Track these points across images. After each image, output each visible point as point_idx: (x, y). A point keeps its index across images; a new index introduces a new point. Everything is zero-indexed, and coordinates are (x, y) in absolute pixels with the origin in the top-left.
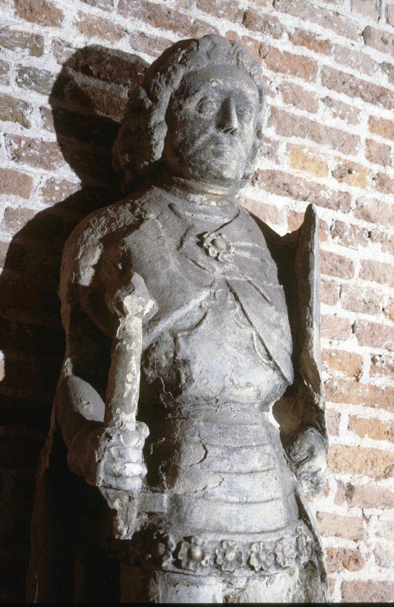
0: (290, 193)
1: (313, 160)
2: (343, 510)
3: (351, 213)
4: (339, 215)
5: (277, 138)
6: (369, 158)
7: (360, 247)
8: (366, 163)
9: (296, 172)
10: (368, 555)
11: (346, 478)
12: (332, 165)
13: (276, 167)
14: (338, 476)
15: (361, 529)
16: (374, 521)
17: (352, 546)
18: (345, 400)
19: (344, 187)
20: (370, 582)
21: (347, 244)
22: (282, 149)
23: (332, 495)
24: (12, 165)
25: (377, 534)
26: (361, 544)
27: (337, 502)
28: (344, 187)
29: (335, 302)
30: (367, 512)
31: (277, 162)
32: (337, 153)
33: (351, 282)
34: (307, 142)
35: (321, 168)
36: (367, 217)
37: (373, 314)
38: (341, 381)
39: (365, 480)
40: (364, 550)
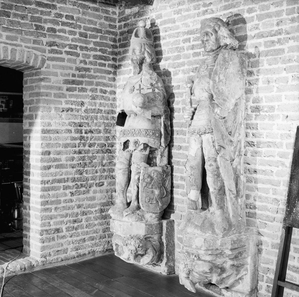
0: (263, 37)
1: (269, 24)
3: (283, 34)
4: (279, 37)
5: (259, 23)
6: (287, 14)
7: (286, 44)
8: (286, 17)
9: (266, 30)
12: (275, 23)
13: (259, 31)
14: (283, 113)
17: (288, 132)
19: (280, 27)
21: (282, 44)
22: (261, 25)
24: (203, 57)
28: (280, 27)
32: (277, 18)
33: (284, 55)
34: (267, 19)
35: (272, 25)
36: (288, 34)
37: (291, 63)
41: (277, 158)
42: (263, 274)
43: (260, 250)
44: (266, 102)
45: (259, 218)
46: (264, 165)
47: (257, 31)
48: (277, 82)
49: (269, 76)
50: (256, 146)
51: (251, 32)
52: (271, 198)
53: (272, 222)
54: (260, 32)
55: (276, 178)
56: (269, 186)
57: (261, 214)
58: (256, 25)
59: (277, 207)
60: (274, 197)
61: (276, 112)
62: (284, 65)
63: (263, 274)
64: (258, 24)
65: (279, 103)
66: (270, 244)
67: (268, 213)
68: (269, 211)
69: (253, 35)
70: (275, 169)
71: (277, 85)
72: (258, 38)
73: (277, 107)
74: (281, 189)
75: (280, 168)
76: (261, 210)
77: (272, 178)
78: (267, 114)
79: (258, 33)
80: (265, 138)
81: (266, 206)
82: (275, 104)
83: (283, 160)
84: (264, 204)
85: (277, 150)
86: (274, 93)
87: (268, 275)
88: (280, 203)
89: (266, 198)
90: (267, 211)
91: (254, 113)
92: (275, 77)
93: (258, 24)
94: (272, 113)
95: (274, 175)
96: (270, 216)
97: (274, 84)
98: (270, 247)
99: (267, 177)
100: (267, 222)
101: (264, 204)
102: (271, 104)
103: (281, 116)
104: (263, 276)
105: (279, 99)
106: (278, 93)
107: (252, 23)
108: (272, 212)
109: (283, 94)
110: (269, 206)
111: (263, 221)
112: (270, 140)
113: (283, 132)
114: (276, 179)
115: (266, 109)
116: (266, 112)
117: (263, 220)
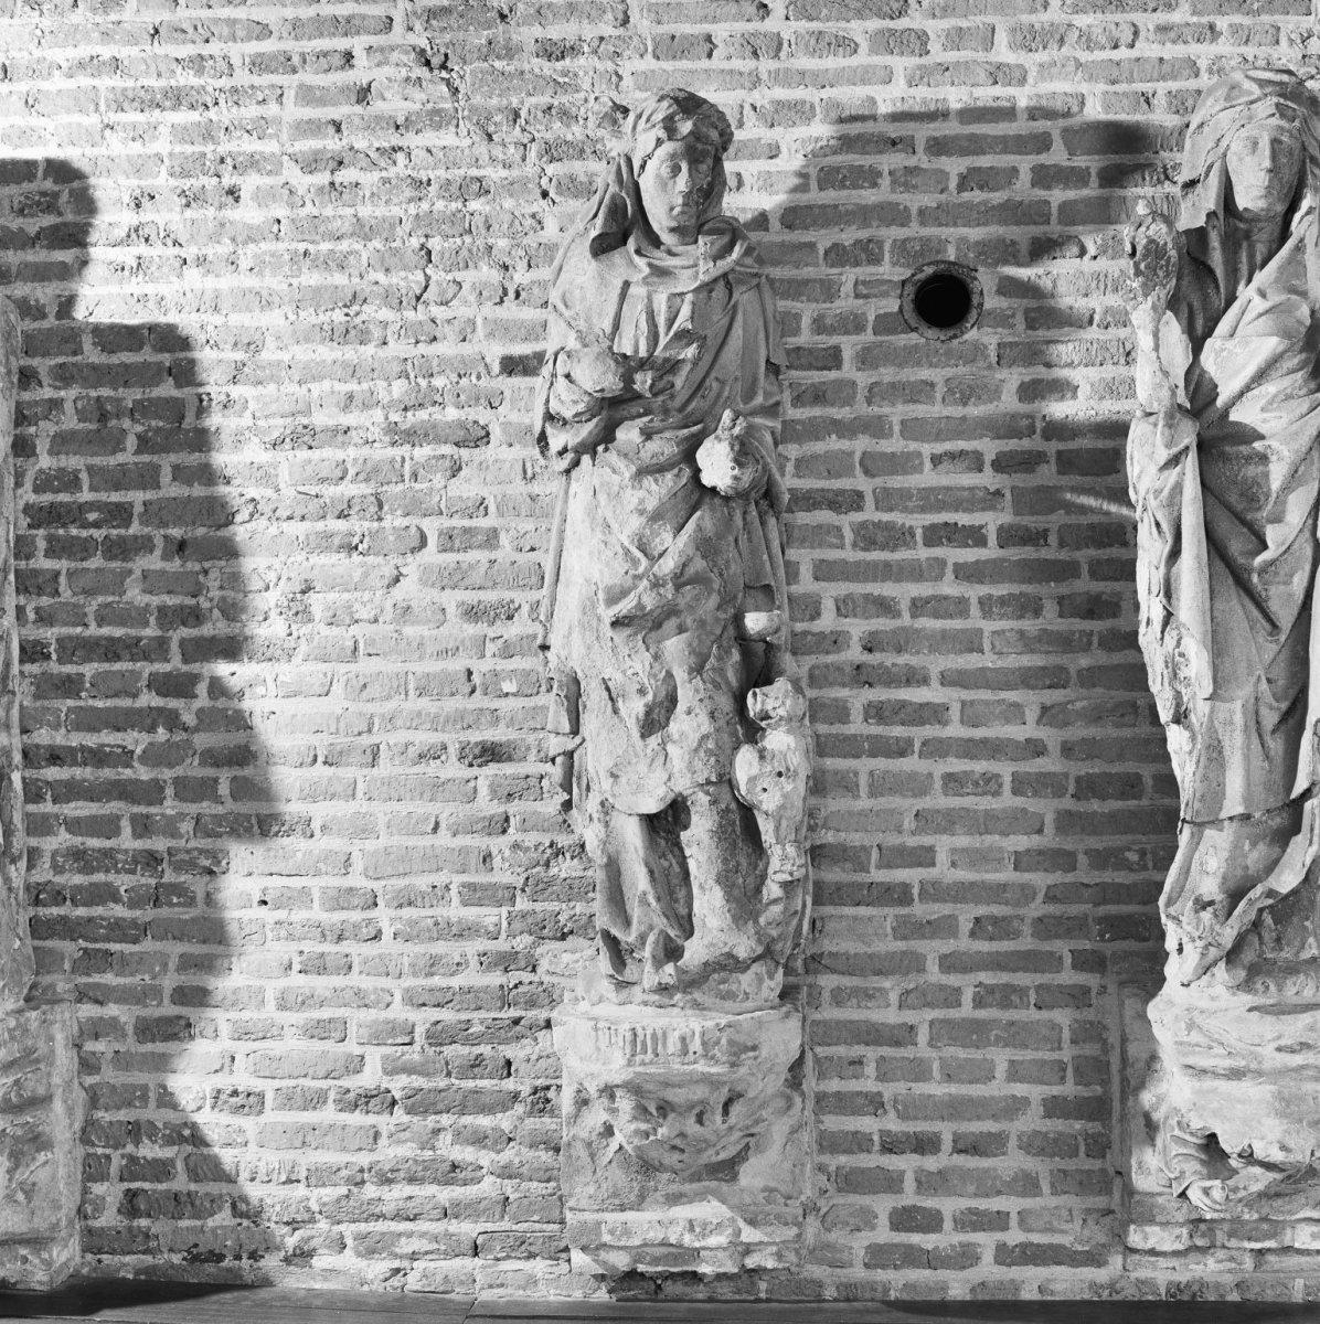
2: (175, 565)
5: (56, 188)
10: (211, 610)
11: (176, 532)
15: (198, 583)
16: (214, 574)
17: (190, 601)
18: (166, 449)
20: (214, 637)
22: (65, 197)
23: (158, 552)
25: (221, 588)
26: (201, 599)
27: (166, 557)
29: (141, 348)
30: (207, 565)
31: (60, 214)
38: (158, 430)
39: (201, 531)
40: (205, 605)
41: (148, 699)
42: (108, 1151)
43: (93, 1061)
44: (92, 488)
45: (81, 936)
46: (93, 729)
47: (48, 220)
48: (137, 416)
49: (105, 392)
50: (54, 657)
51: (21, 220)
52: (126, 851)
53: (135, 941)
54: (65, 224)
55: (144, 774)
56: (114, 807)
57: (90, 920)
58: (43, 194)
59: (153, 882)
60: (139, 844)
61: (135, 528)
62: (167, 355)
63: (108, 1151)
64: (56, 195)
65: (149, 495)
66: (130, 1030)
67: (119, 911)
68: (116, 899)
69: (32, 230)
70: (136, 741)
71: (139, 428)
72: (51, 247)
73: (138, 509)
74: (169, 812)
75: (162, 734)
76: (85, 905)
77: (127, 773)
78: (98, 534)
79: (55, 228)
80: (93, 625)
81: (108, 885)
82: (137, 497)
83: (173, 703)
84: (99, 877)
85: (146, 669)
86: (127, 457)
87: (130, 1148)
88: (165, 865)
89: (108, 853)
90: (112, 905)
91: (41, 532)
92: (131, 395)
93: (56, 195)
94: (123, 531)
95: (136, 764)
96: (124, 919)
97: (126, 423)
98: (131, 1039)
99: (107, 773)
100: (115, 947)
101: (99, 877)
102: (115, 497)
103: (159, 542)
104: (108, 1157)
105: (148, 478)
106: (146, 458)
107: (25, 185)
108: (132, 905)
109: (166, 462)
110: (123, 882)
111: (98, 946)
112: (118, 632)
113: (171, 601)
114: (145, 777)
115: (92, 516)
116: (96, 525)
117: (96, 941)
